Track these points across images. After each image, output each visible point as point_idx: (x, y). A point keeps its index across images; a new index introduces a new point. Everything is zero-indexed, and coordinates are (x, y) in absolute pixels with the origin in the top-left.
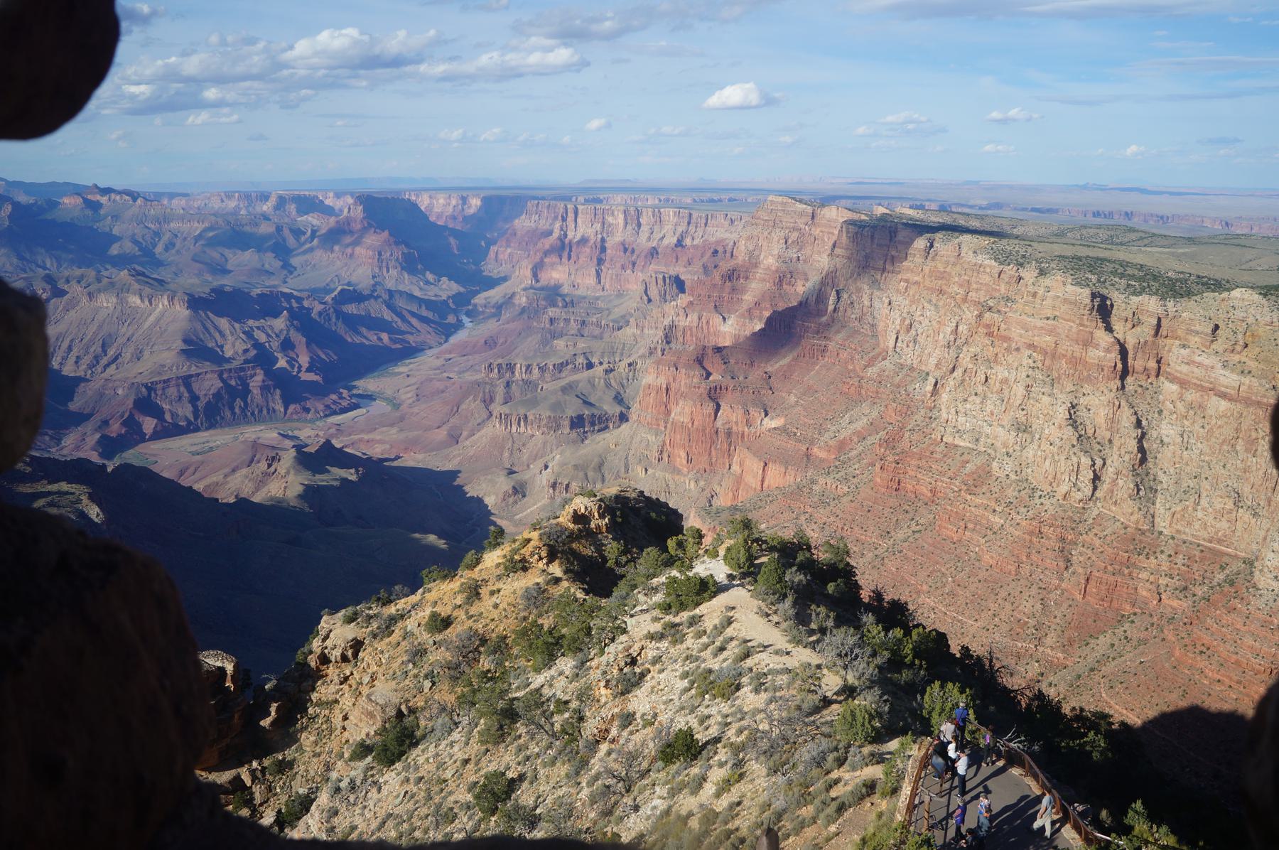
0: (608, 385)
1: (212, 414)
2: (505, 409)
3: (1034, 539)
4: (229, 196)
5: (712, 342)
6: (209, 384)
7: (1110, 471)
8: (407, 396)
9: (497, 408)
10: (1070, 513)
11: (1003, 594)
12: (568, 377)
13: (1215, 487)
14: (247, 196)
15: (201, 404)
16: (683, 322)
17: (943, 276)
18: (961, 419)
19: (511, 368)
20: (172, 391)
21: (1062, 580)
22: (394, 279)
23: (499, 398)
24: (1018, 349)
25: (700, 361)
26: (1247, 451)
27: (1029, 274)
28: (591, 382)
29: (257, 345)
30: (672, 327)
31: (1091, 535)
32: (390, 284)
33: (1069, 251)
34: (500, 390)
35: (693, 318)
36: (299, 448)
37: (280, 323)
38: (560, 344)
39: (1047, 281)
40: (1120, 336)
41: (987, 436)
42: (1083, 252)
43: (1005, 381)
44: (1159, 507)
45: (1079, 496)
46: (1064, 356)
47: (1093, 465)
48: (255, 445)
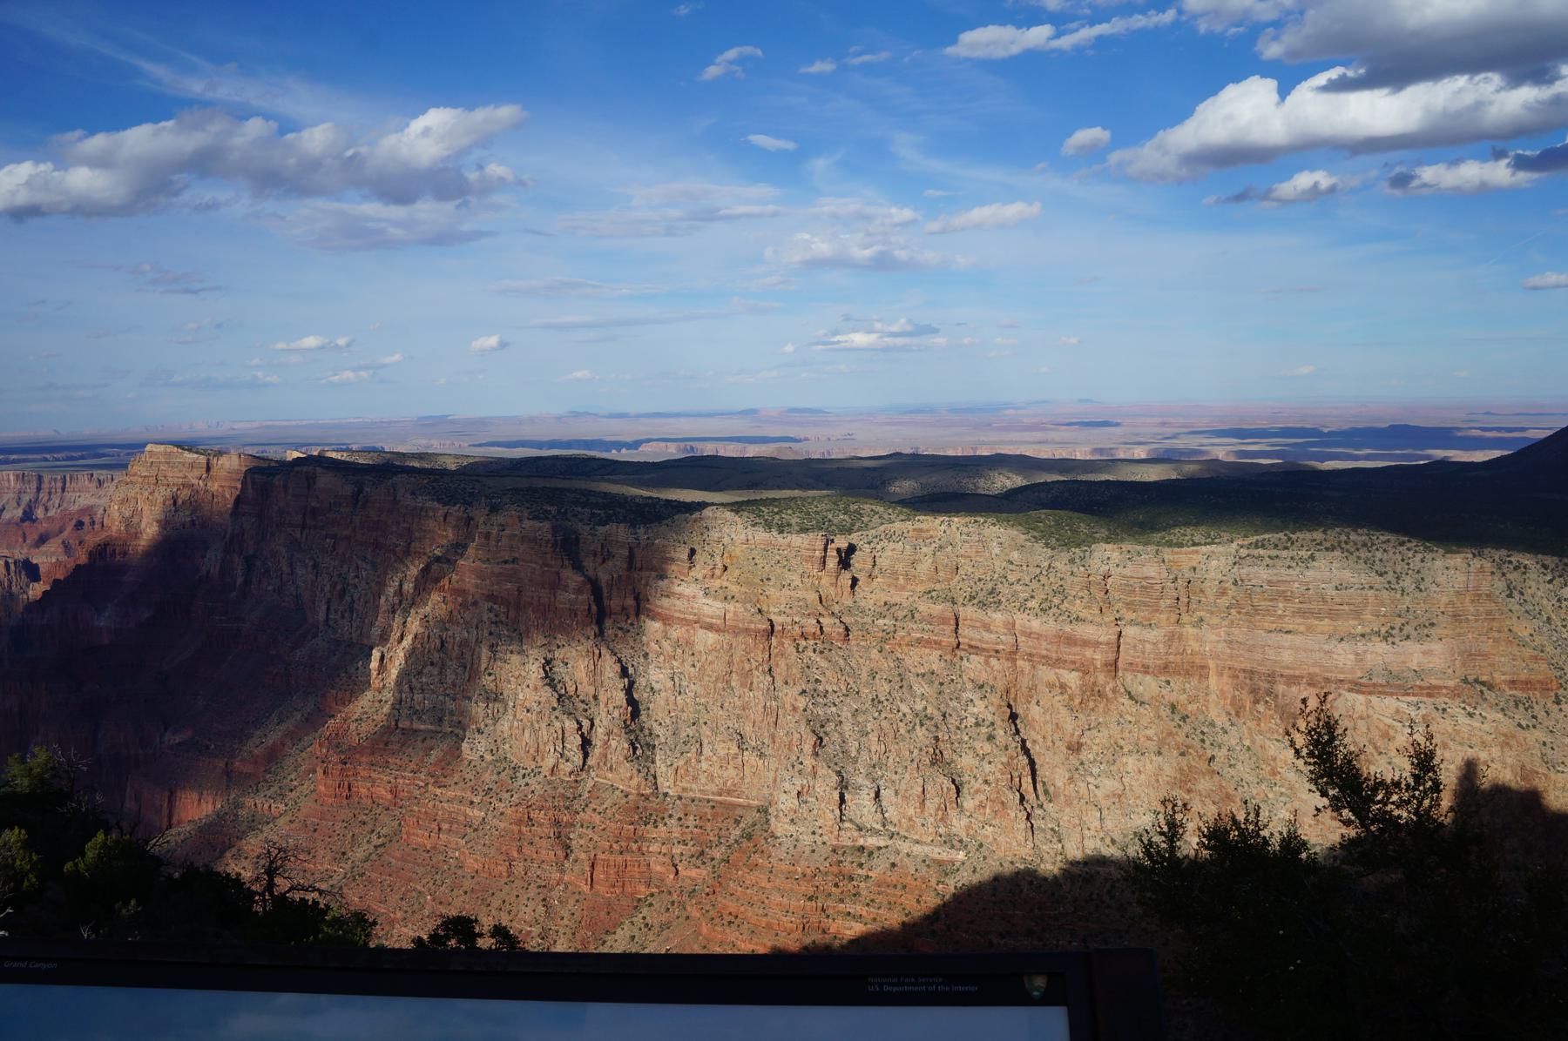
3: (524, 829)
7: (600, 731)
10: (561, 790)
11: (496, 903)
13: (715, 731)
18: (418, 697)
21: (563, 872)
24: (475, 603)
26: (743, 685)
27: (480, 515)
31: (589, 810)
33: (524, 483)
39: (501, 519)
40: (591, 573)
41: (452, 713)
42: (540, 483)
43: (464, 643)
44: (660, 766)
45: (568, 767)
46: (530, 604)
47: (580, 728)
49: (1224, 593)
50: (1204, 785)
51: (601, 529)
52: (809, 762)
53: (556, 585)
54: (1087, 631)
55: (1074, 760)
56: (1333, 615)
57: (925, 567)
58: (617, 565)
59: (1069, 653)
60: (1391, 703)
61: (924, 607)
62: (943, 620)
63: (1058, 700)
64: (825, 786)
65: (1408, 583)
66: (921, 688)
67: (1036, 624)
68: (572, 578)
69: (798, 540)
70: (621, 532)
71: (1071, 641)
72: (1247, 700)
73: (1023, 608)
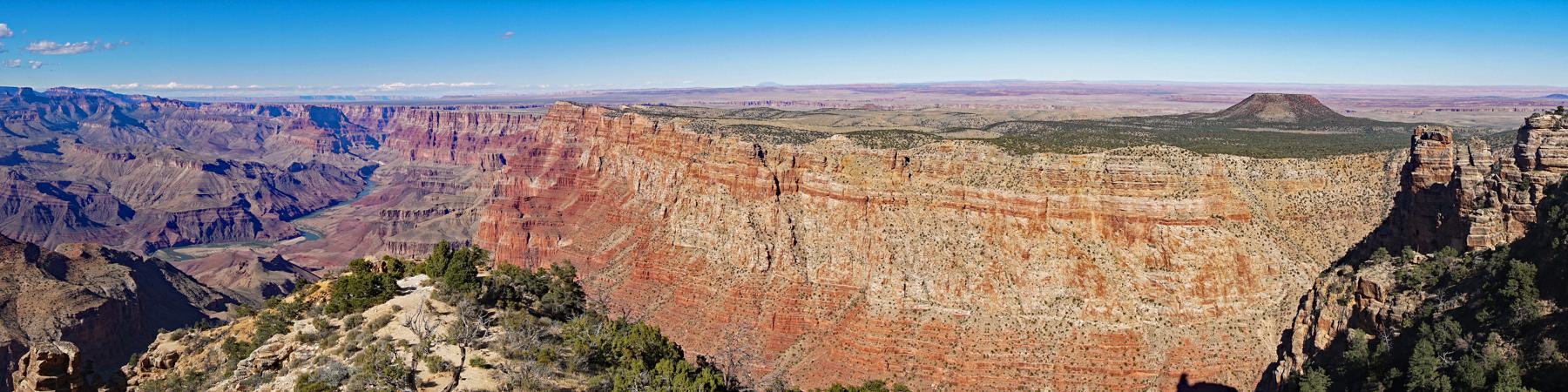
0: (459, 224)
1: (209, 235)
2: (392, 239)
4: (233, 105)
5: (525, 194)
6: (210, 218)
8: (331, 231)
9: (388, 238)
12: (433, 219)
14: (243, 106)
15: (205, 228)
16: (505, 183)
17: (665, 143)
19: (397, 213)
20: (189, 219)
22: (326, 157)
23: (389, 232)
25: (516, 206)
28: (447, 221)
29: (241, 195)
30: (499, 186)
32: (324, 161)
34: (390, 227)
35: (512, 180)
36: (261, 259)
37: (256, 182)
38: (428, 197)
39: (727, 140)
48: (235, 255)
49: (1098, 177)
50: (1090, 272)
51: (779, 147)
52: (887, 267)
53: (755, 175)
54: (1032, 197)
55: (1026, 263)
56: (1152, 186)
57: (946, 167)
58: (786, 165)
59: (1024, 209)
60: (1179, 228)
61: (947, 186)
62: (957, 193)
63: (1018, 233)
64: (896, 279)
65: (1186, 171)
66: (946, 228)
67: (1005, 195)
68: (763, 171)
69: (881, 152)
70: (789, 148)
71: (1022, 202)
72: (1110, 229)
73: (998, 186)
